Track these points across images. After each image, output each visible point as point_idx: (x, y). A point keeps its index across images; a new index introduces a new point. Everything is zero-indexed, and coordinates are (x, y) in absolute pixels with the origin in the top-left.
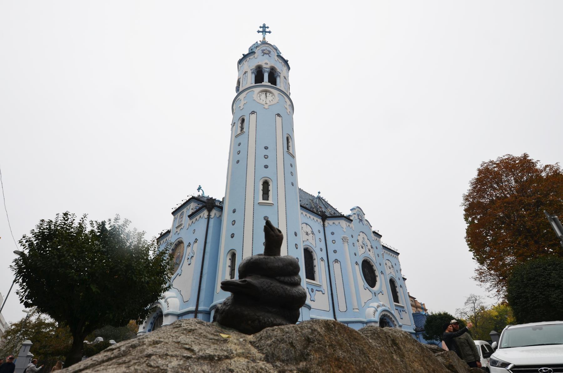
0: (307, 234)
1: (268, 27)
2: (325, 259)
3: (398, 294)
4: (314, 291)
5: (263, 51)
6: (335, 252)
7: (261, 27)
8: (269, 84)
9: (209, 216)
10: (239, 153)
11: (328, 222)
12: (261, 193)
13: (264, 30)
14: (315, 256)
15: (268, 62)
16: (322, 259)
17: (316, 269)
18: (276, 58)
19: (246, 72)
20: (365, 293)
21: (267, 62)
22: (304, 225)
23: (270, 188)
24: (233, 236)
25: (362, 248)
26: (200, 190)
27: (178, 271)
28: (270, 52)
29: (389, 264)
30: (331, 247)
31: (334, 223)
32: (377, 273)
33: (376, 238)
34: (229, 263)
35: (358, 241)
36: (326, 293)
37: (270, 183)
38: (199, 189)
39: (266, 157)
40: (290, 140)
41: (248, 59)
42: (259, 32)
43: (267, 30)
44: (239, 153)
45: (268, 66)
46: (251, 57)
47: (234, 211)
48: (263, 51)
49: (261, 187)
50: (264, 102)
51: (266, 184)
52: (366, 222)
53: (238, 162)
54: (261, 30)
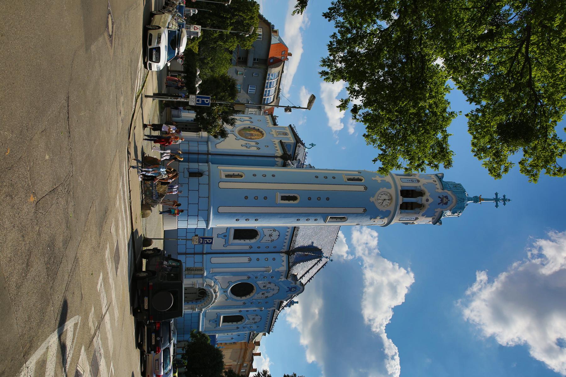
1: (504, 204)
2: (252, 250)
3: (230, 323)
5: (446, 197)
7: (504, 196)
8: (400, 202)
9: (277, 157)
11: (284, 257)
12: (287, 195)
13: (509, 200)
15: (429, 202)
16: (251, 247)
17: (242, 241)
18: (439, 210)
19: (418, 181)
22: (277, 233)
25: (264, 286)
26: (311, 146)
28: (446, 204)
32: (244, 298)
33: (276, 303)
34: (236, 173)
35: (270, 283)
37: (295, 202)
38: (312, 145)
39: (319, 199)
40: (343, 220)
41: (437, 183)
42: (496, 194)
43: (501, 203)
45: (424, 201)
46: (439, 186)
48: (446, 197)
49: (291, 195)
51: (294, 198)
52: (290, 295)
53: (317, 177)
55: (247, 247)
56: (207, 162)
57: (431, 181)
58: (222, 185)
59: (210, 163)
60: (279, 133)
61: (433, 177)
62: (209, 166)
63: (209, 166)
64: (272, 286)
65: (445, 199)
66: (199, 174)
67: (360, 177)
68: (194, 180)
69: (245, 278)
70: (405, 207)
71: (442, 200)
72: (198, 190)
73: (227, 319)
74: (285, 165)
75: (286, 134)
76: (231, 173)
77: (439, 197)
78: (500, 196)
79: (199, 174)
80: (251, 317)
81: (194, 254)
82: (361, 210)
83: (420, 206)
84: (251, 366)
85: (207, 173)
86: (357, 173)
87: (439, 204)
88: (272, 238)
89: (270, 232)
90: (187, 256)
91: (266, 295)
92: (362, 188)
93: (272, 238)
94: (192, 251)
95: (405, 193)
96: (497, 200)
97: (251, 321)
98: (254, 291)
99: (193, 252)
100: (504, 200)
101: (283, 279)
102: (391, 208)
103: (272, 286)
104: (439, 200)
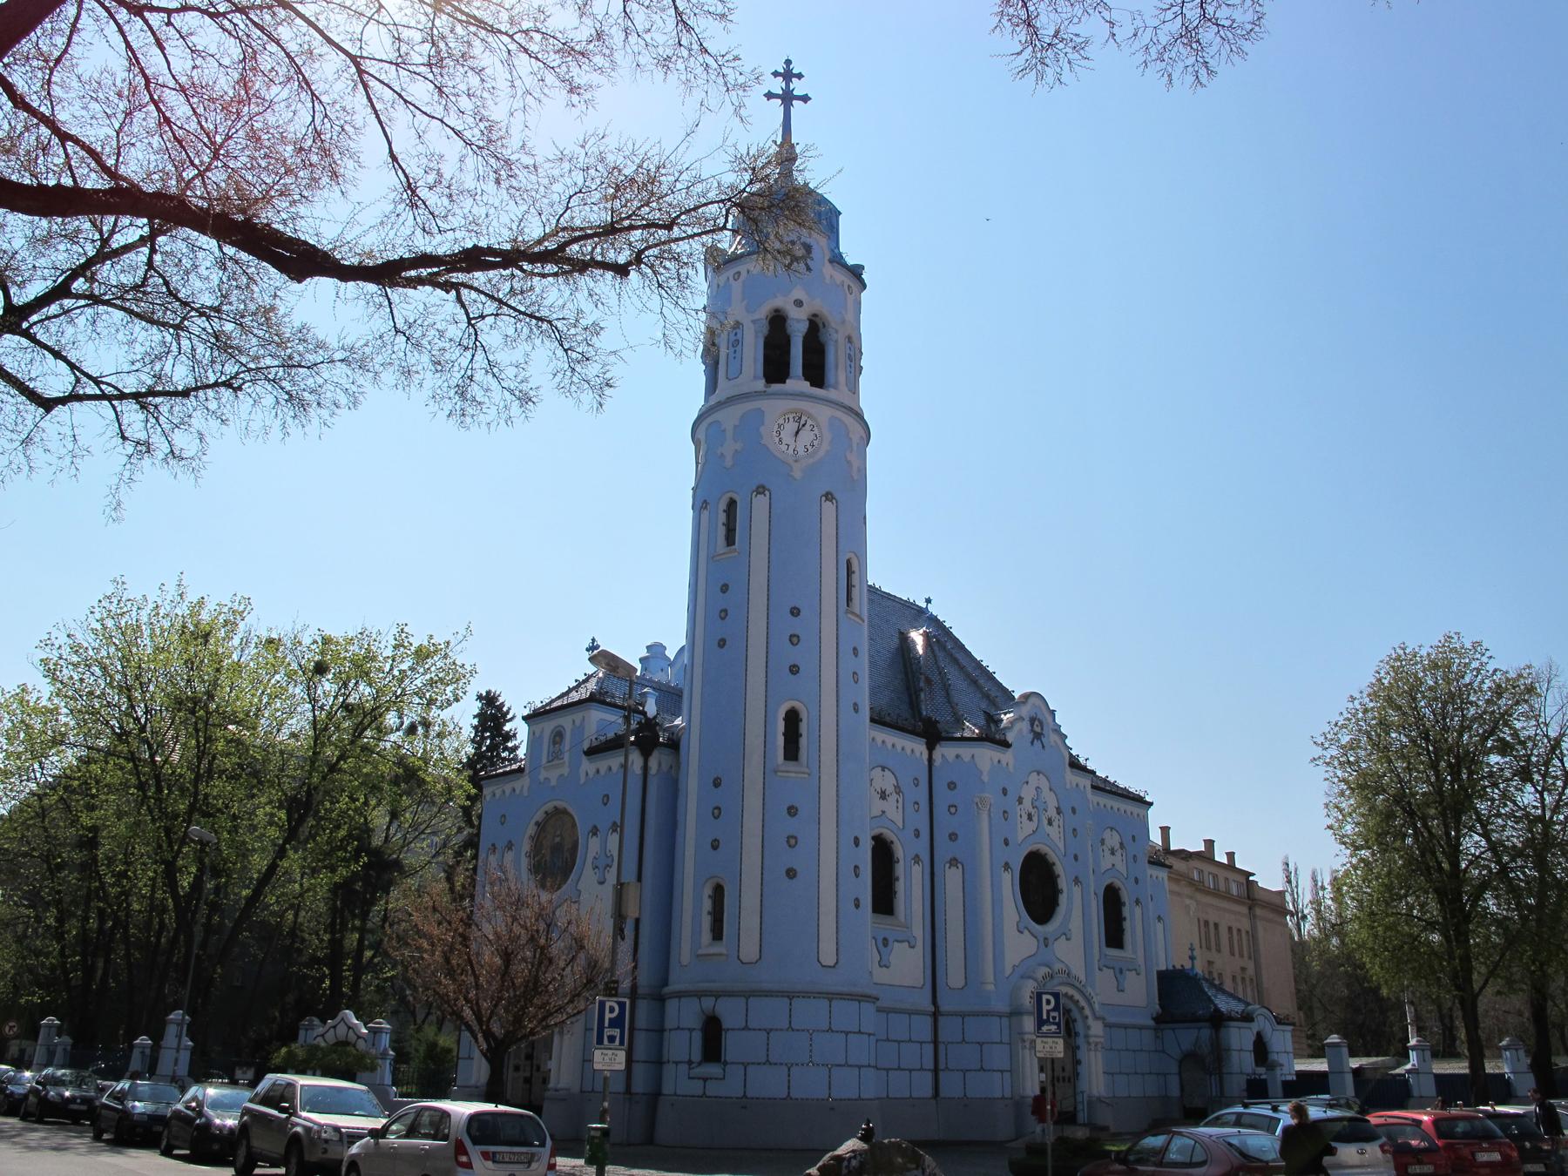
0: (883, 795)
1: (800, 76)
2: (926, 857)
3: (1127, 925)
4: (891, 940)
8: (805, 386)
9: (645, 768)
10: (724, 614)
11: (945, 752)
12: (781, 740)
14: (899, 852)
16: (917, 859)
17: (900, 887)
19: (738, 325)
20: (1016, 940)
21: (799, 300)
23: (803, 727)
24: (715, 845)
25: (1030, 818)
29: (1113, 840)
30: (945, 823)
31: (957, 756)
32: (1063, 883)
34: (707, 905)
35: (1020, 801)
36: (920, 944)
37: (804, 715)
39: (794, 639)
40: (855, 567)
43: (798, 87)
44: (724, 614)
47: (717, 783)
50: (791, 451)
51: (792, 718)
52: (1054, 737)
53: (722, 643)
54: (777, 86)
55: (917, 870)
56: (660, 999)
57: (737, 287)
58: (749, 949)
59: (666, 990)
60: (555, 756)
61: (723, 279)
62: (679, 995)
63: (679, 995)
64: (1028, 794)
66: (712, 1031)
67: (723, 505)
68: (732, 1045)
69: (1007, 876)
70: (816, 373)
72: (769, 1031)
73: (1114, 935)
74: (674, 745)
75: (558, 736)
76: (706, 921)
78: (777, 86)
79: (712, 1031)
80: (1107, 861)
81: (936, 1042)
82: (829, 508)
83: (815, 328)
84: (1198, 854)
85: (708, 1003)
86: (705, 514)
88: (890, 789)
90: (942, 1066)
91: (1052, 812)
92: (761, 503)
93: (890, 789)
95: (776, 369)
96: (787, 98)
97: (1118, 859)
98: (1044, 849)
100: (788, 75)
101: (1007, 757)
102: (823, 413)
103: (1028, 794)
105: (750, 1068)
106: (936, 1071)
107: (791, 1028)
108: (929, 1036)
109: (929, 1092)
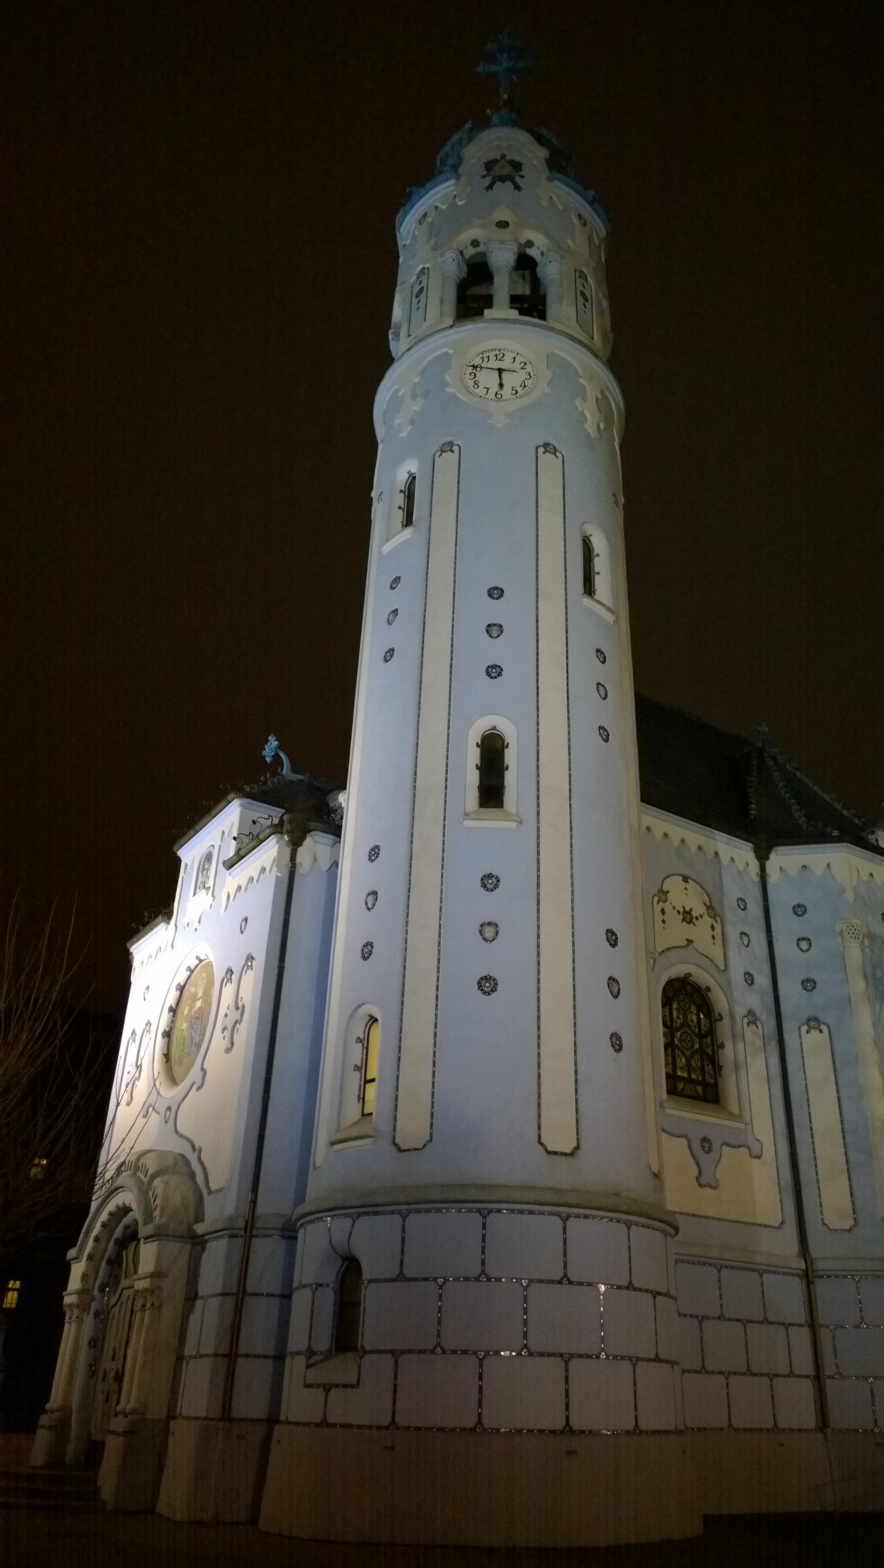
0: (688, 917)
4: (716, 1144)
5: (489, 166)
6: (809, 984)
8: (514, 314)
12: (473, 778)
22: (674, 885)
27: (194, 1074)
28: (517, 166)
49: (474, 756)
65: (497, 170)
71: (503, 179)
77: (490, 187)
81: (812, 1324)
87: (517, 187)
88: (699, 910)
89: (674, 919)
90: (829, 1368)
93: (699, 910)
94: (801, 1338)
99: (806, 1332)
104: (503, 189)
105: (404, 1361)
106: (818, 1378)
107: (483, 1276)
108: (799, 1315)
109: (808, 1418)
